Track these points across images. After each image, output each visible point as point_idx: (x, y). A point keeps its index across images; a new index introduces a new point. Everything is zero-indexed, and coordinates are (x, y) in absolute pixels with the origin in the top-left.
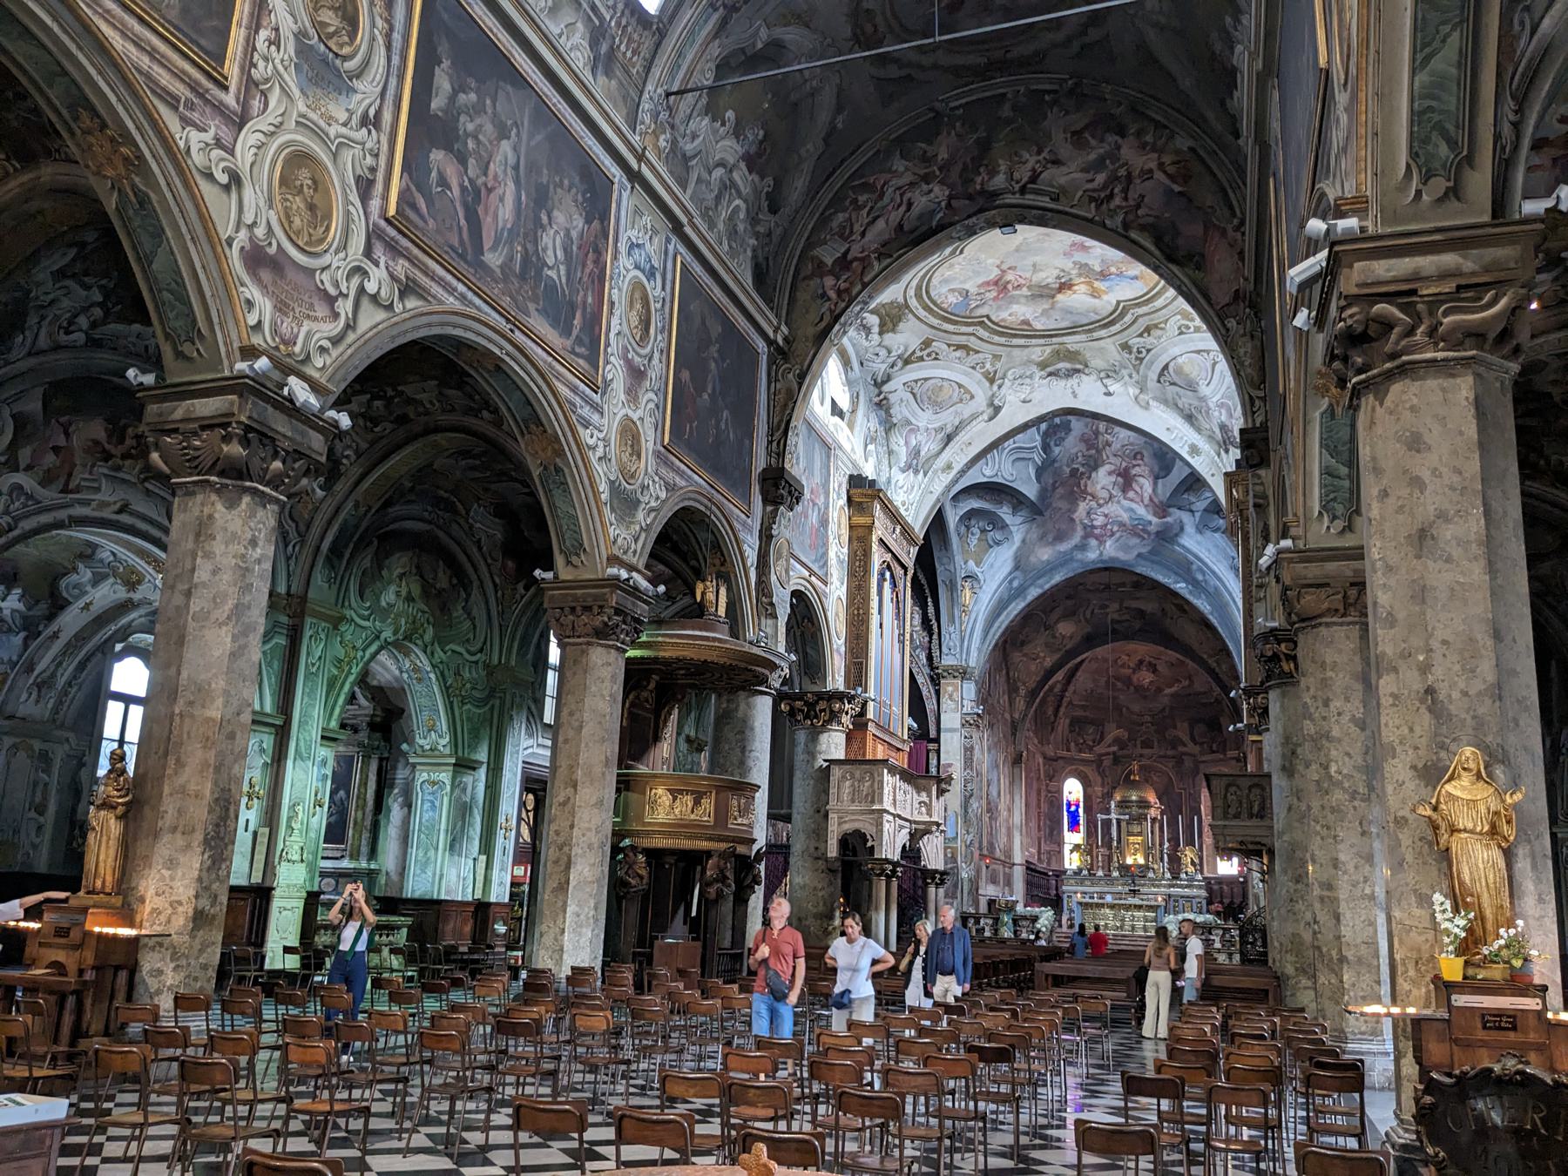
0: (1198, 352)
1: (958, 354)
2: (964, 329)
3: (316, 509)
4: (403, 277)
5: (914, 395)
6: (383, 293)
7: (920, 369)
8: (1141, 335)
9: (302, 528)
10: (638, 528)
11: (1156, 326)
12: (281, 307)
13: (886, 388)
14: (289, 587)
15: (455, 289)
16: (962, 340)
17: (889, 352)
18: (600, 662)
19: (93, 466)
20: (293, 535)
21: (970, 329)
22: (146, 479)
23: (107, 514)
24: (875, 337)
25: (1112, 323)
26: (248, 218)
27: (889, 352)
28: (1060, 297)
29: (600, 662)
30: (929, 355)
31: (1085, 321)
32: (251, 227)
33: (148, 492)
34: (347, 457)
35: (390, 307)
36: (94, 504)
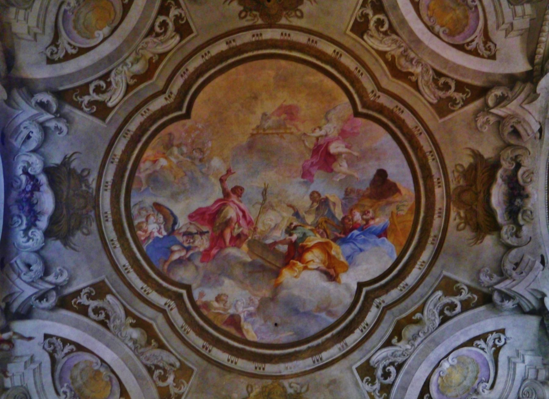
0: (470, 343)
1: (136, 334)
2: (154, 297)
5: (54, 362)
7: (77, 326)
8: (388, 343)
11: (409, 321)
13: (20, 327)
16: (147, 314)
17: (47, 272)
21: (161, 300)
24: (38, 235)
25: (349, 330)
27: (47, 272)
28: (287, 275)
30: (97, 311)
31: (314, 329)
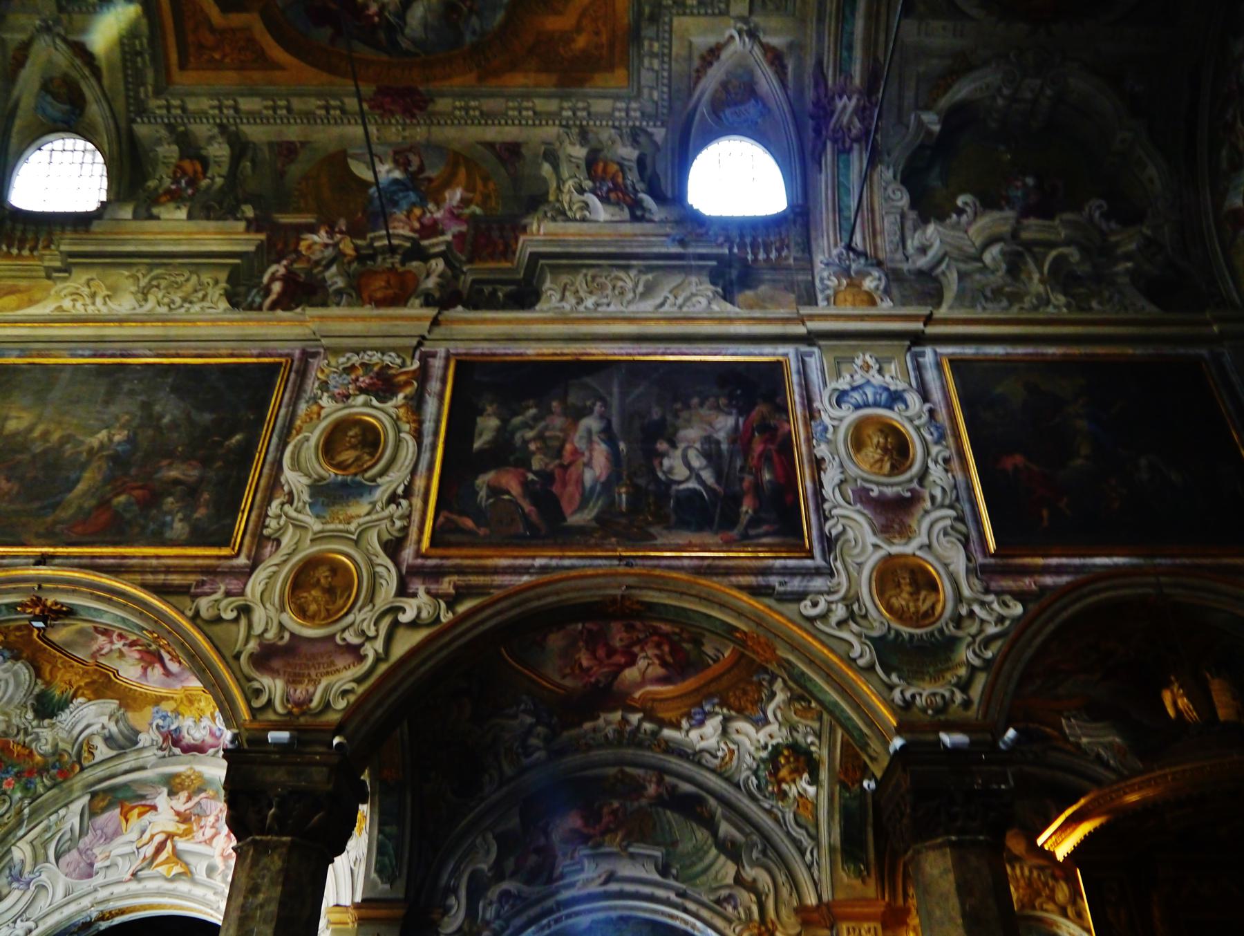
3: (816, 806)
4: (452, 591)
6: (424, 615)
9: (812, 831)
10: (963, 671)
12: (294, 680)
14: (820, 897)
15: (532, 566)
18: (936, 872)
19: (574, 851)
20: (807, 843)
22: (629, 845)
23: (594, 888)
26: (258, 629)
29: (936, 872)
32: (261, 636)
33: (632, 856)
34: (812, 743)
35: (437, 620)
36: (579, 884)
